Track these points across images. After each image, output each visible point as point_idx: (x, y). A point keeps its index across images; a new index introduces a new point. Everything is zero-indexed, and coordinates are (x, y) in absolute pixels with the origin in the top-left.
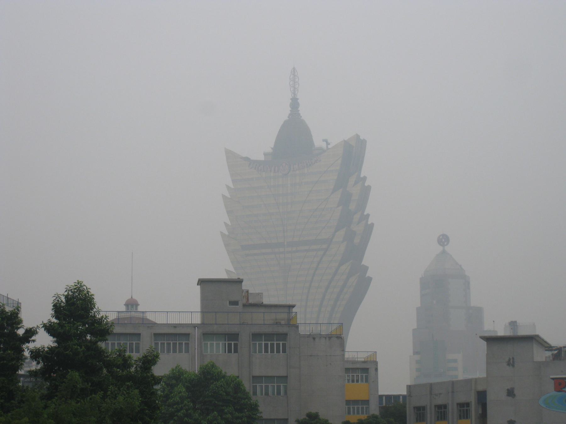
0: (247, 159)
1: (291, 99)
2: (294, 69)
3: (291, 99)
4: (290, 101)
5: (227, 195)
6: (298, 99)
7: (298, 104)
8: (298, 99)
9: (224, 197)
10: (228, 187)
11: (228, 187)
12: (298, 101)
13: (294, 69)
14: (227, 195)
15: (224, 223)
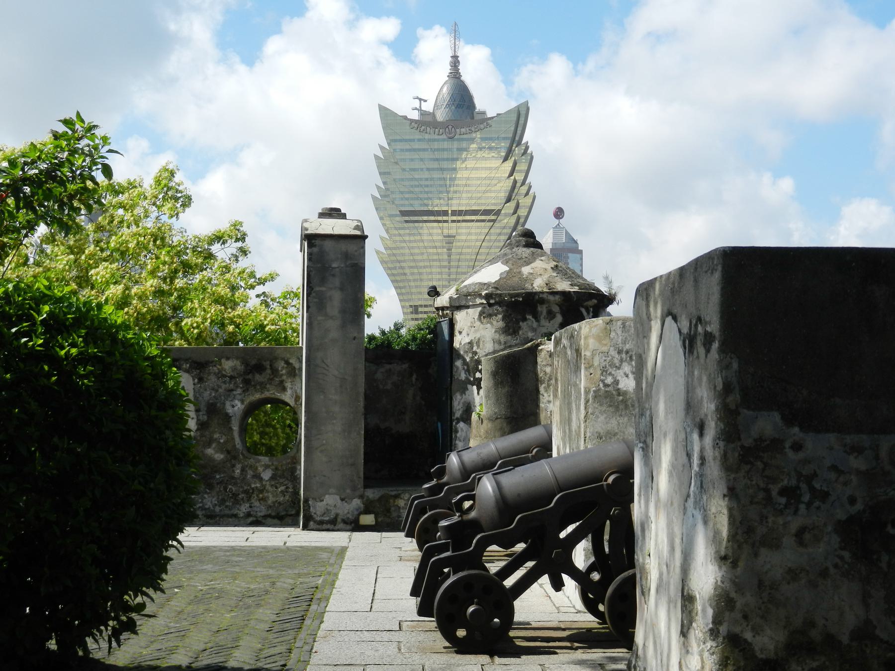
0: (405, 118)
1: (452, 57)
2: (456, 24)
3: (452, 57)
4: (451, 59)
5: (380, 155)
6: (458, 57)
7: (459, 62)
8: (458, 57)
9: (376, 157)
10: (382, 148)
11: (382, 148)
12: (459, 59)
13: (456, 24)
14: (380, 155)
15: (376, 185)
